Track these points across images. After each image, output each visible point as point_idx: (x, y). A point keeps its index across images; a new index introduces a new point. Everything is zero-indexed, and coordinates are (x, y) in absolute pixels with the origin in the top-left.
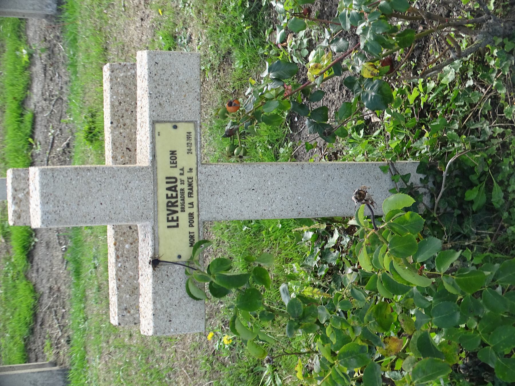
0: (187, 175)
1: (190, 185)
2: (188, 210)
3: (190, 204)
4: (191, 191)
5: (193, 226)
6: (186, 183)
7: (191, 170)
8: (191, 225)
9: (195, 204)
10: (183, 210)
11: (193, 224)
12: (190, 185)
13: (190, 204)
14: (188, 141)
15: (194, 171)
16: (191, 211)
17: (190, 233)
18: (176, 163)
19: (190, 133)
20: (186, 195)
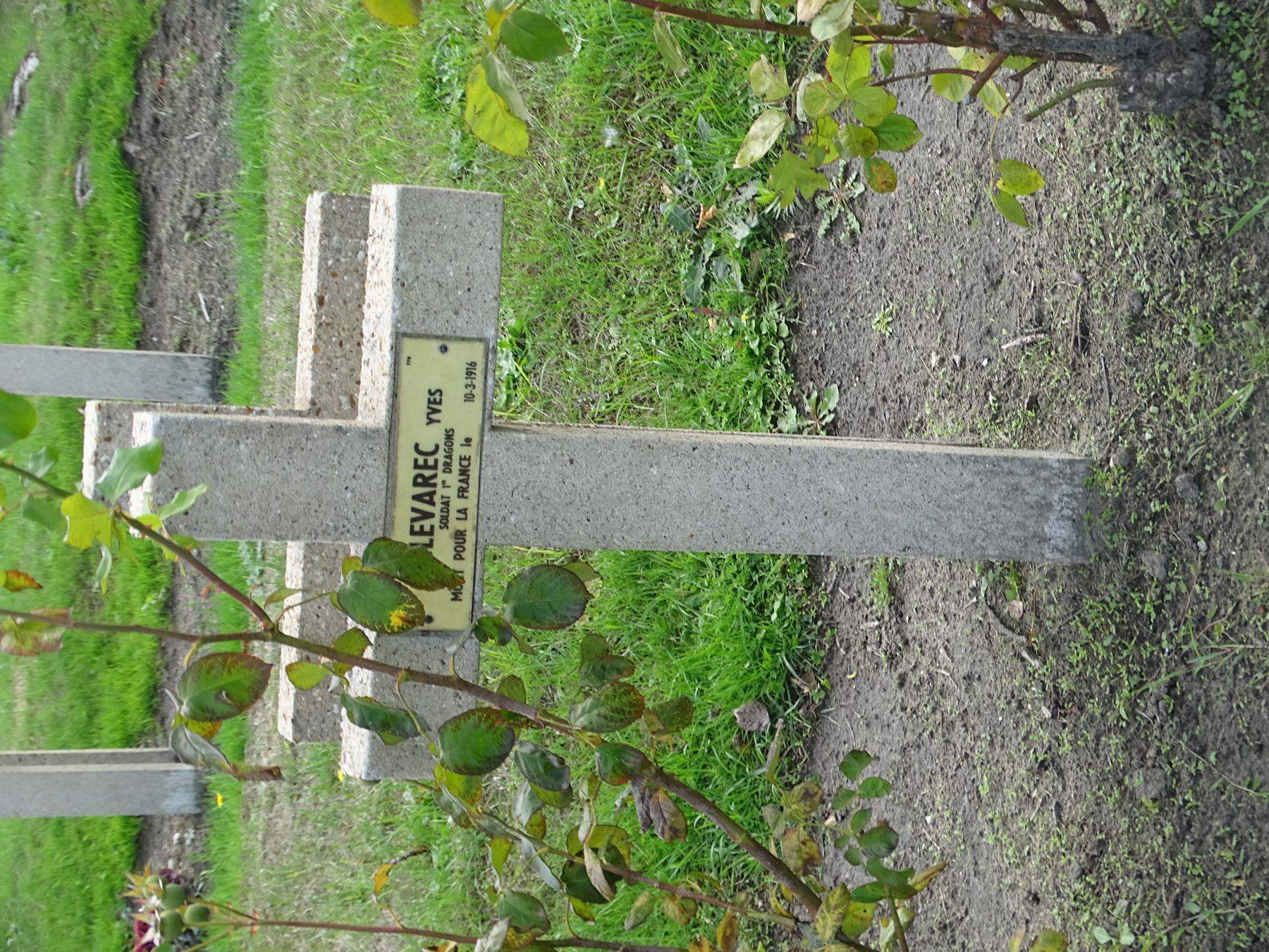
1: (464, 472)
2: (455, 524)
3: (459, 511)
4: (464, 485)
5: (462, 558)
6: (456, 467)
7: (468, 441)
9: (472, 512)
10: (445, 523)
11: (463, 555)
12: (464, 472)
13: (459, 511)
14: (469, 382)
15: (475, 443)
16: (460, 526)
19: (473, 364)
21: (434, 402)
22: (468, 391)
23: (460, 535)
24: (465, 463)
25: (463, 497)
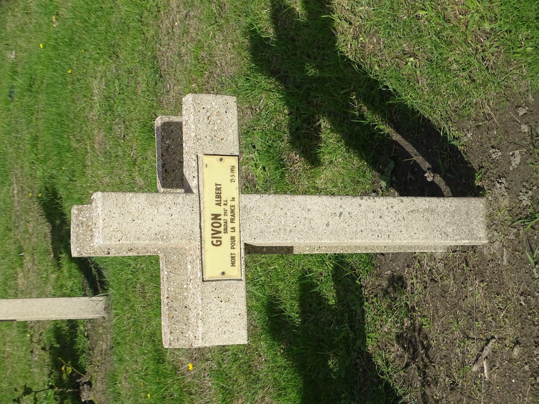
0: (230, 203)
1: (232, 211)
2: (230, 234)
3: (232, 228)
5: (234, 248)
7: (233, 199)
8: (233, 248)
9: (237, 229)
12: (232, 211)
13: (232, 228)
14: (232, 174)
15: (237, 200)
16: (233, 234)
17: (231, 254)
18: (221, 198)
20: (229, 221)
21: (218, 189)
22: (232, 178)
23: (233, 238)
24: (233, 208)
25: (233, 222)
